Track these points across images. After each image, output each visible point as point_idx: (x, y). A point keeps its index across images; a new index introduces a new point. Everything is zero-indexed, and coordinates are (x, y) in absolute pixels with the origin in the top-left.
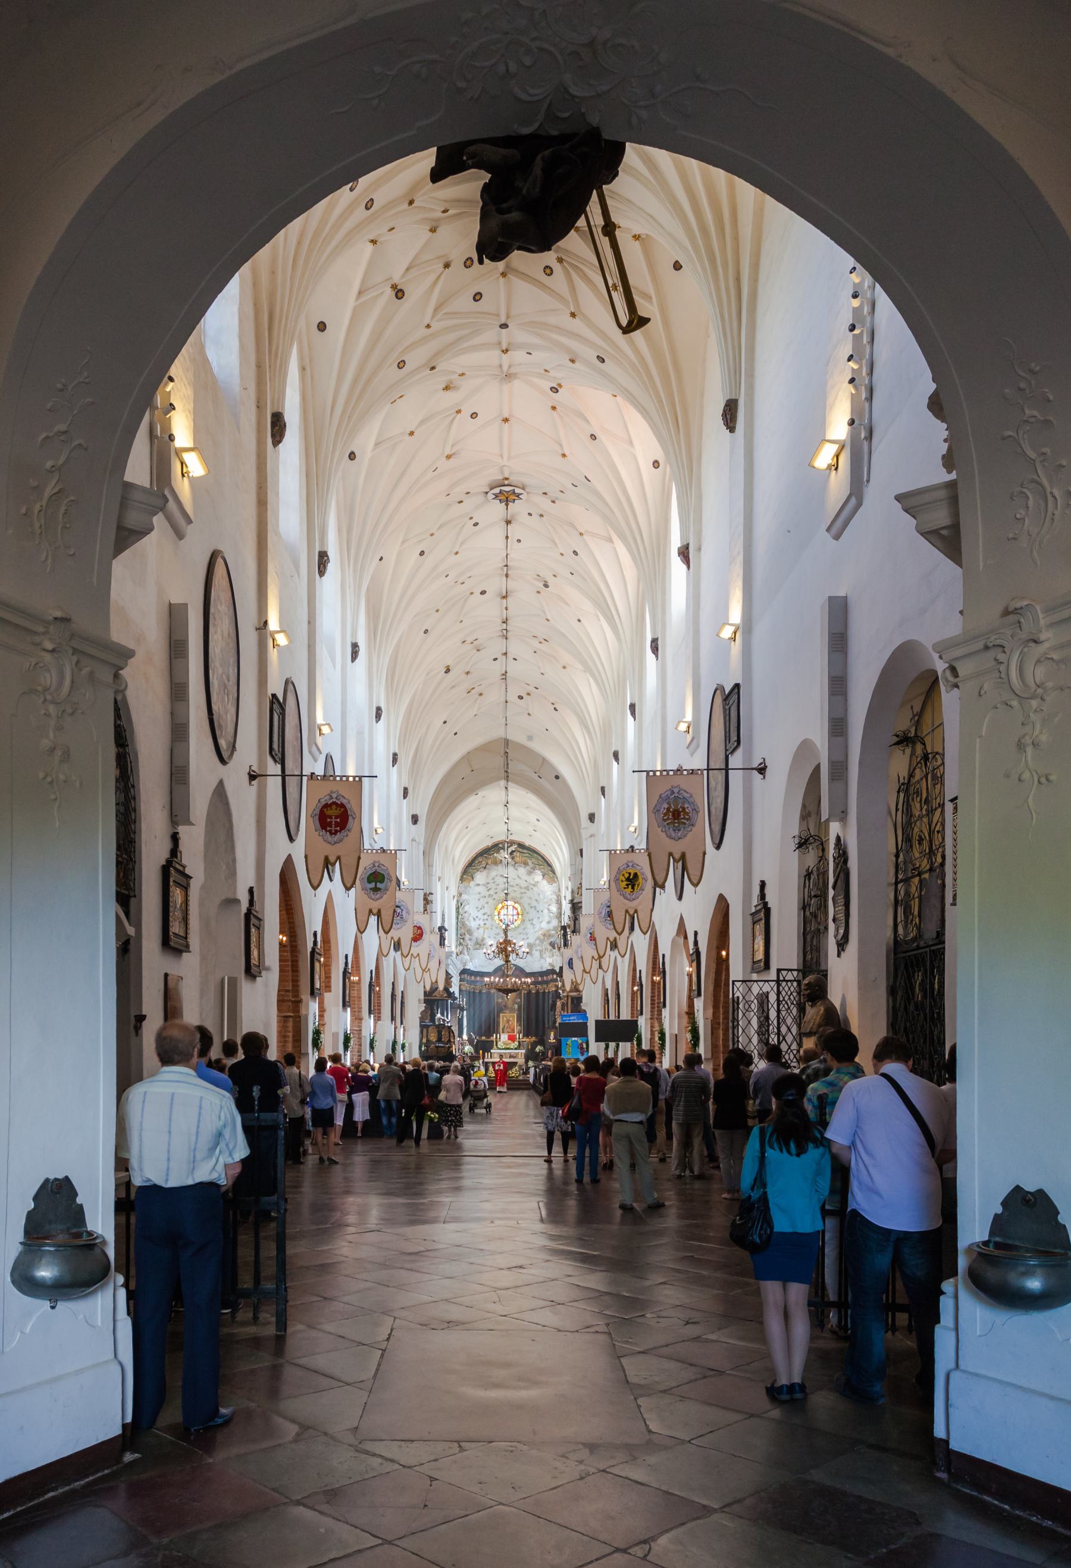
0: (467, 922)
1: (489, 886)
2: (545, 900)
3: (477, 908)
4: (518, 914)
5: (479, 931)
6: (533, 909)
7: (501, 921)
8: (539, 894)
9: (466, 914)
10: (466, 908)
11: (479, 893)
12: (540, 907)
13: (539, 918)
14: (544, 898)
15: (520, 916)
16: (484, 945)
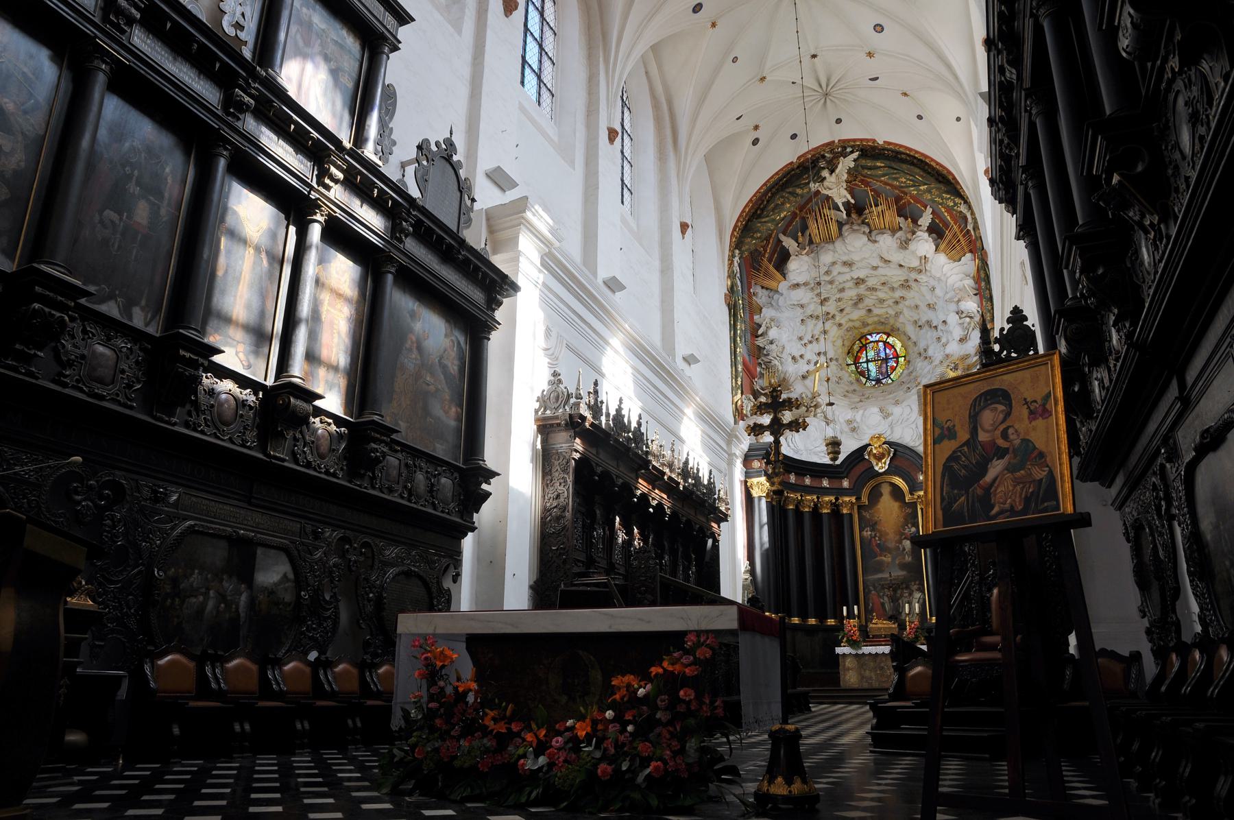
0: (776, 362)
1: (825, 291)
2: (948, 296)
3: (801, 339)
4: (897, 357)
5: (808, 382)
6: (927, 327)
7: (862, 374)
8: (934, 289)
9: (773, 346)
10: (773, 334)
11: (802, 306)
12: (936, 319)
13: (939, 339)
14: (947, 293)
15: (902, 360)
16: (816, 406)
